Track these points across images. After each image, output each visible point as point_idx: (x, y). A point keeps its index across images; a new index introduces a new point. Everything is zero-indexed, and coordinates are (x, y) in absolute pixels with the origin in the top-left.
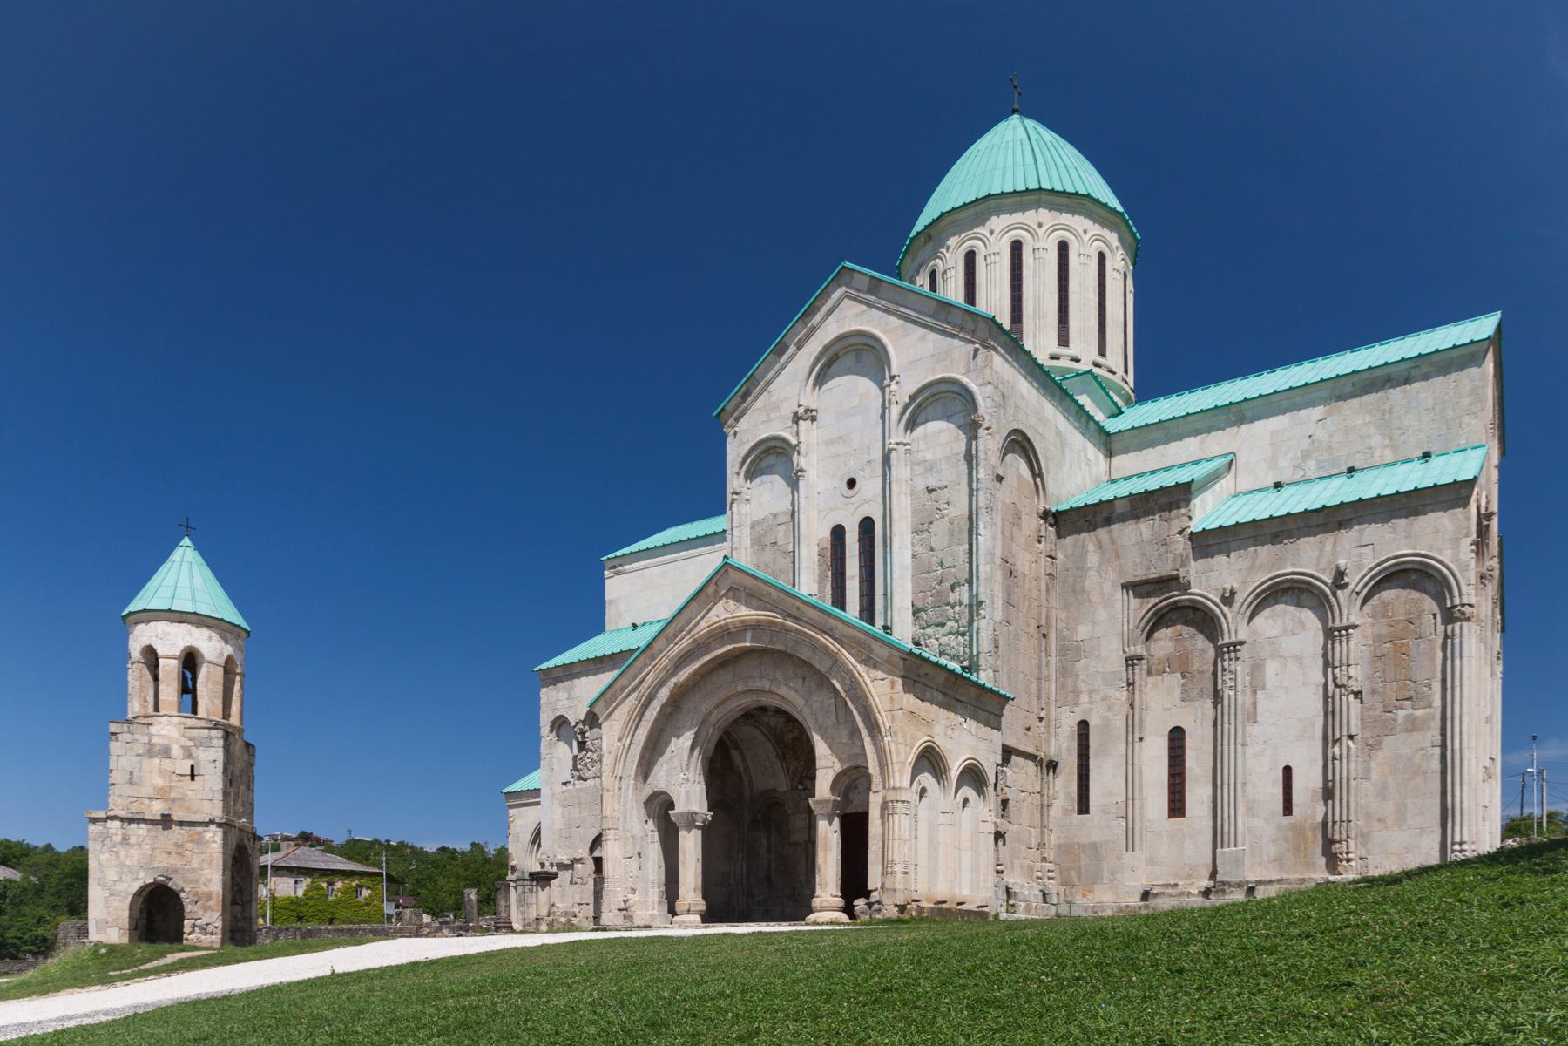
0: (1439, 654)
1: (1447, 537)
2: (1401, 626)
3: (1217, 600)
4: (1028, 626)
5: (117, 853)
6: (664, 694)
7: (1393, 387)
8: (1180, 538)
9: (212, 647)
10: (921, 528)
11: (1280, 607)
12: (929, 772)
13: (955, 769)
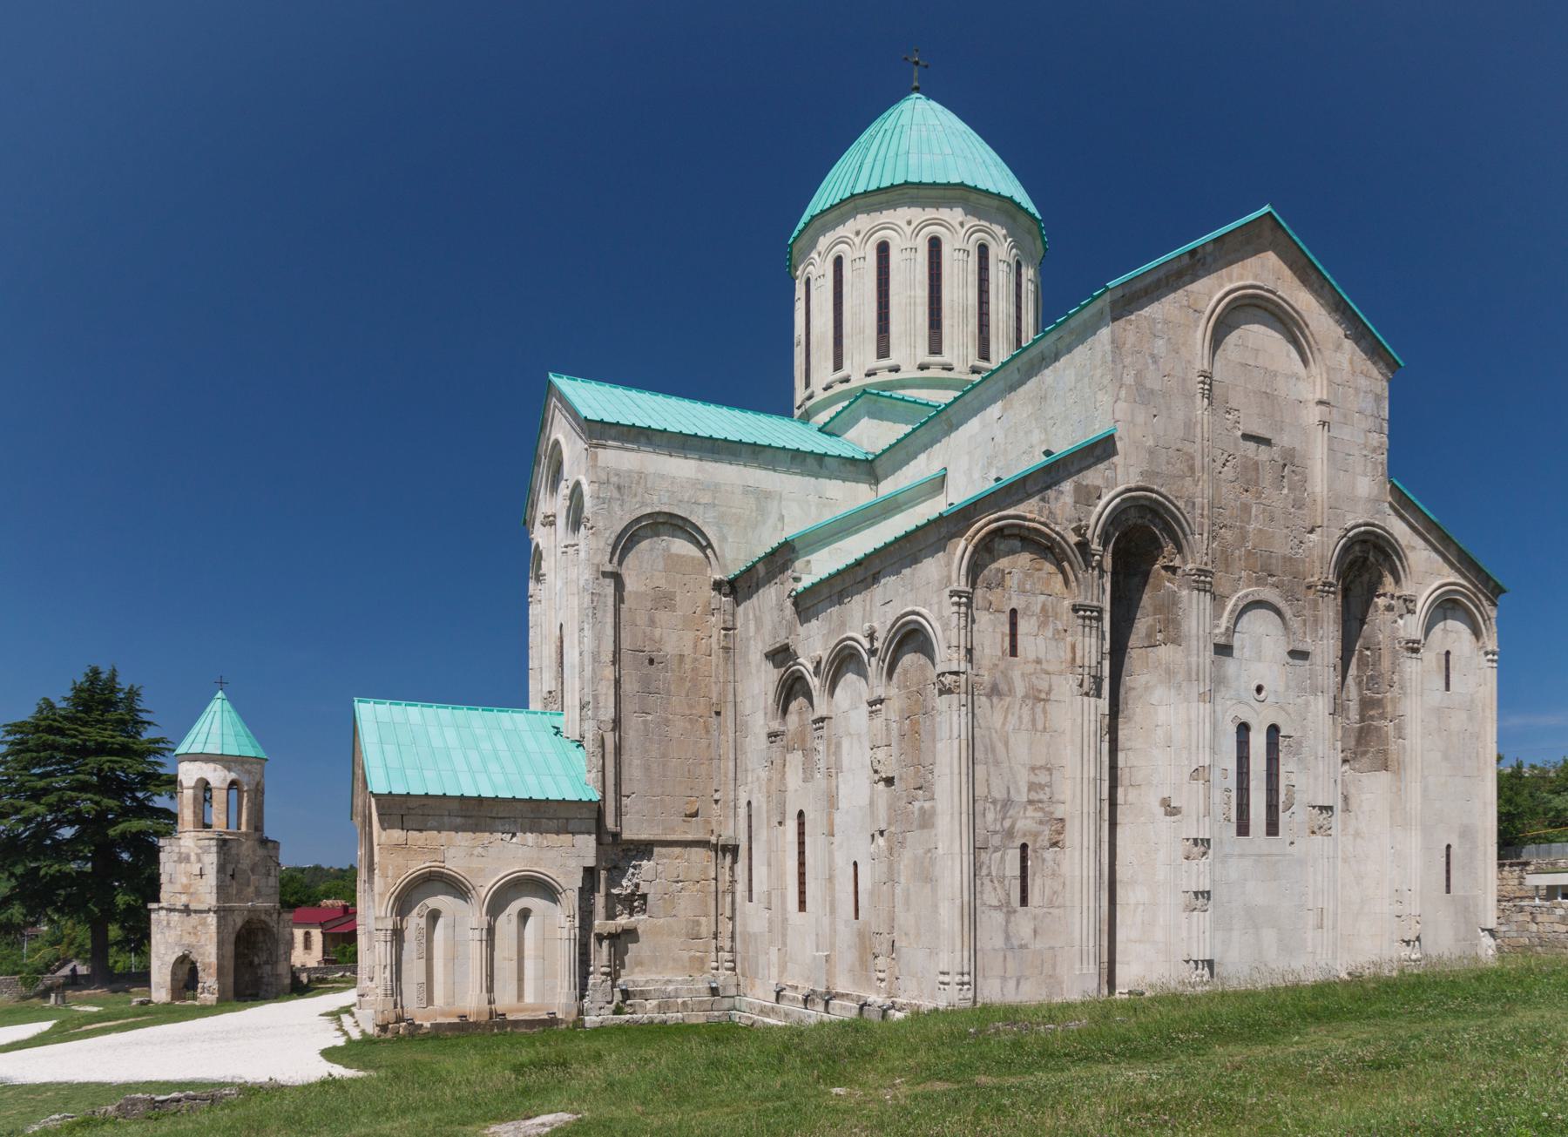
1: (935, 589)
2: (914, 698)
3: (811, 670)
4: (691, 707)
7: (1047, 367)
9: (217, 776)
12: (446, 893)
13: (485, 887)
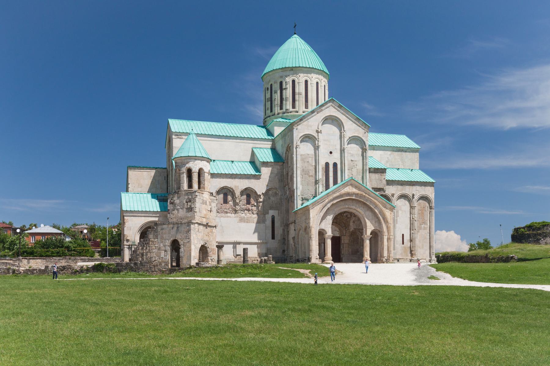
0: (429, 215)
6: (329, 205)
8: (384, 180)
10: (350, 169)
11: (401, 199)
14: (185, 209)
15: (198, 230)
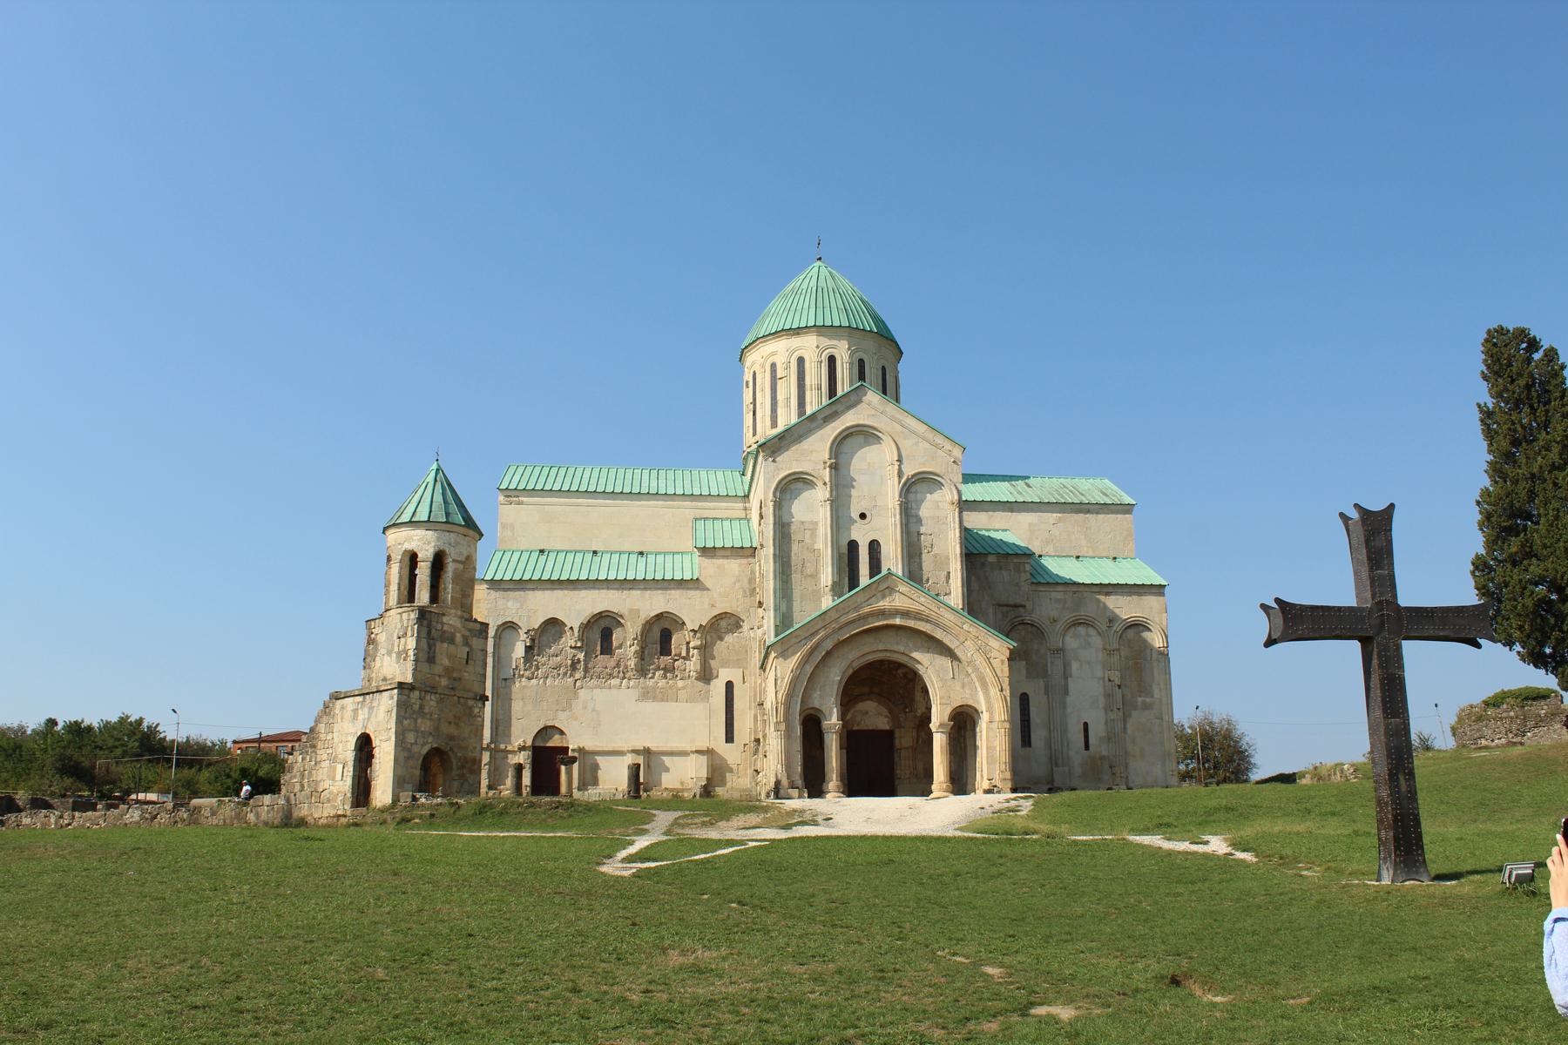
5: (416, 721)
6: (829, 645)
14: (394, 655)
15: (422, 707)
